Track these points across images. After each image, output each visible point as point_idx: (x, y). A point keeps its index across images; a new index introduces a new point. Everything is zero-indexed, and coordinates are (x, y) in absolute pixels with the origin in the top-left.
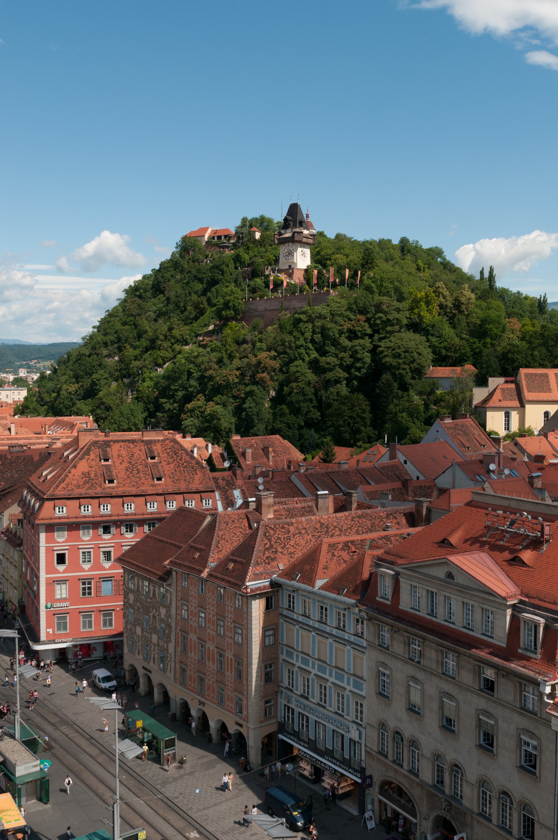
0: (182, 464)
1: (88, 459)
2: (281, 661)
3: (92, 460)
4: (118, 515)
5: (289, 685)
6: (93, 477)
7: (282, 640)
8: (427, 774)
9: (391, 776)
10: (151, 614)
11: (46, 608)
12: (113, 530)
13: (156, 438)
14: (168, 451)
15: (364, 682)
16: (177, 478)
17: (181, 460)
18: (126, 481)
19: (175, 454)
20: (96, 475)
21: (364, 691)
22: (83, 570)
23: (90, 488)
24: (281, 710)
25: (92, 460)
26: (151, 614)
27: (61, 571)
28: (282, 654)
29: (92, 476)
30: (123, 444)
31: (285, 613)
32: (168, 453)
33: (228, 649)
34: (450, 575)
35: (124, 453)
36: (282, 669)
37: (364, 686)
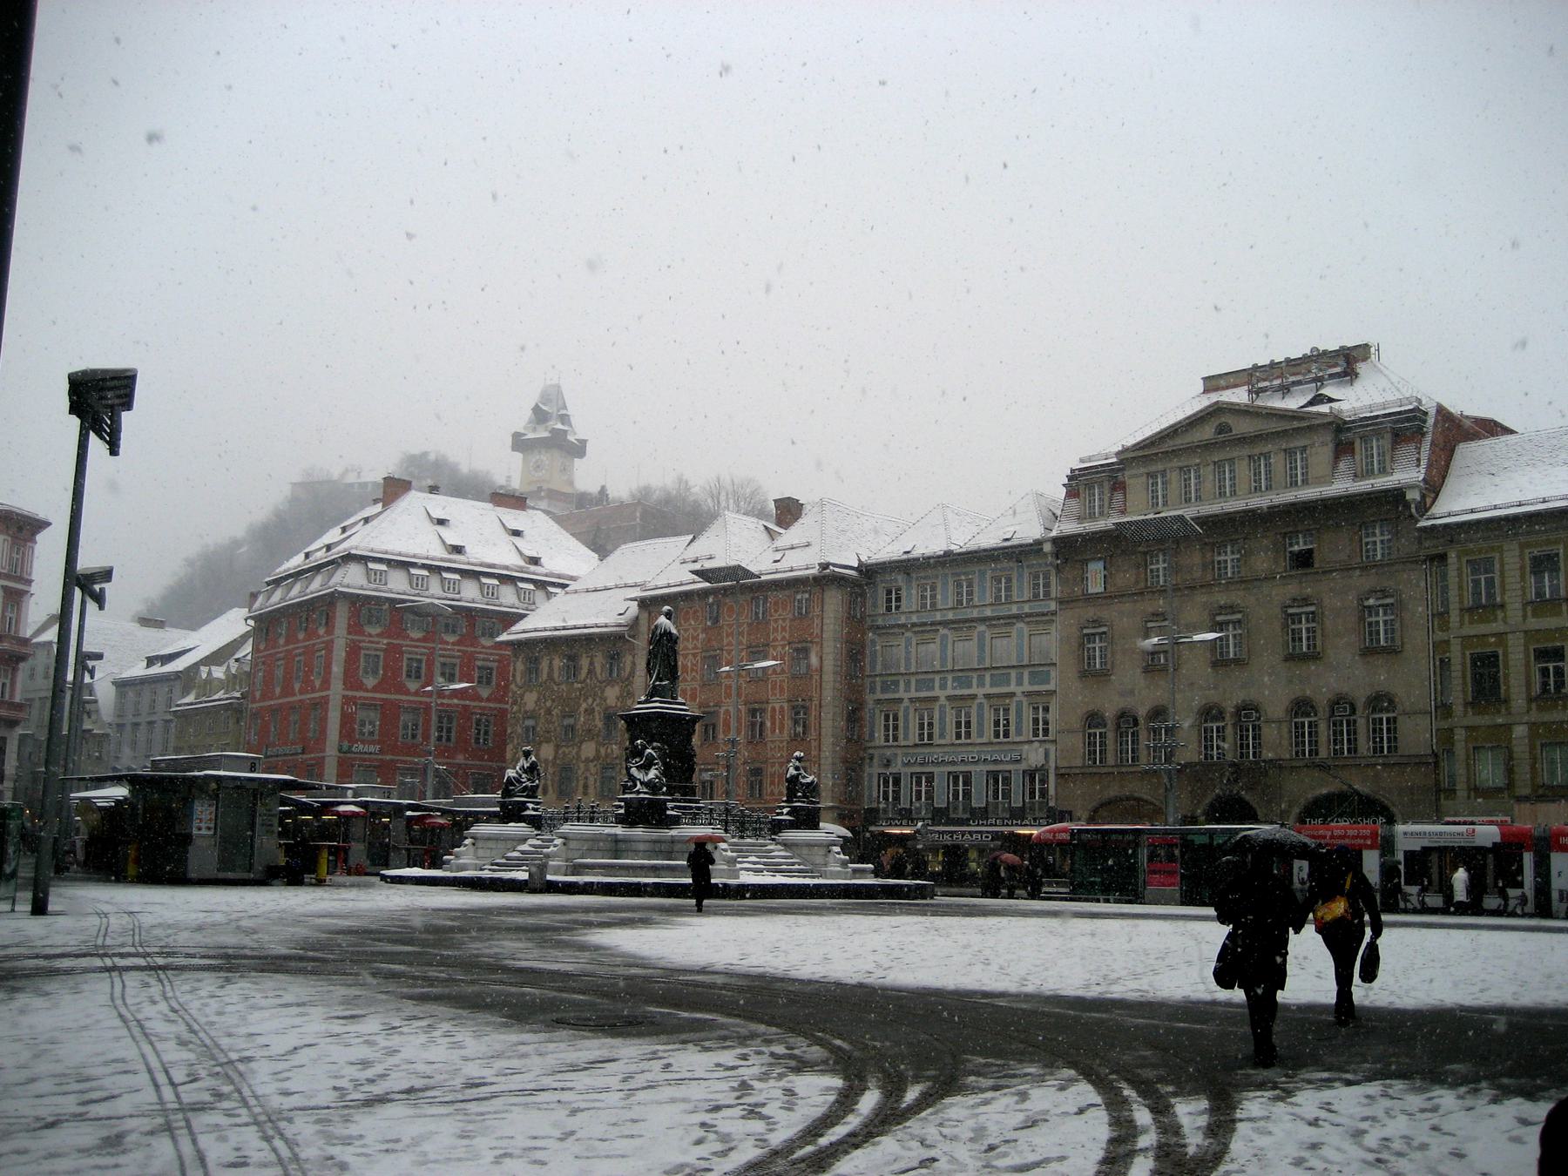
2: (870, 704)
7: (873, 668)
11: (340, 751)
15: (1051, 668)
21: (1053, 682)
22: (407, 692)
24: (870, 788)
28: (873, 690)
34: (1223, 429)
36: (873, 717)
37: (1053, 674)
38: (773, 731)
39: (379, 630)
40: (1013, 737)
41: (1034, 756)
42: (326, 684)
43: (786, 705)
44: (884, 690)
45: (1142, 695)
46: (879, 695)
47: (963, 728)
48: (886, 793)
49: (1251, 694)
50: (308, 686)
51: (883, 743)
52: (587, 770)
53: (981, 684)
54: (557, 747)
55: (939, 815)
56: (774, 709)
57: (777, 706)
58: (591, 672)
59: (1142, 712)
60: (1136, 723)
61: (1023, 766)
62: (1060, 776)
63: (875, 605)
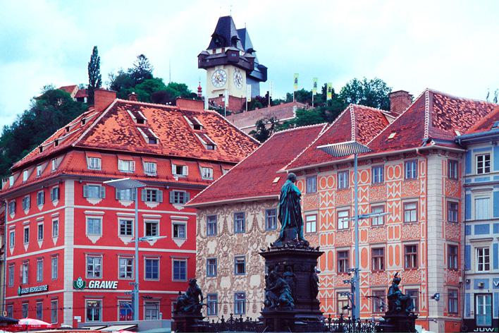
0: (234, 139)
1: (116, 118)
3: (122, 120)
4: (167, 179)
5: (481, 268)
6: (128, 135)
10: (249, 252)
11: (75, 286)
12: (160, 194)
13: (196, 111)
14: (214, 124)
16: (231, 150)
17: (231, 134)
18: (170, 144)
19: (223, 129)
20: (131, 134)
22: (122, 244)
23: (127, 144)
24: (469, 304)
25: (122, 120)
26: (249, 252)
27: (94, 242)
29: (127, 134)
30: (156, 110)
31: (473, 181)
32: (214, 127)
33: (391, 236)
35: (161, 119)
38: (391, 264)
39: (98, 201)
42: (61, 242)
43: (400, 245)
44: (476, 233)
46: (473, 236)
48: (482, 307)
50: (48, 244)
51: (477, 271)
52: (255, 294)
54: (233, 280)
56: (391, 247)
57: (394, 246)
58: (255, 223)
63: (468, 170)
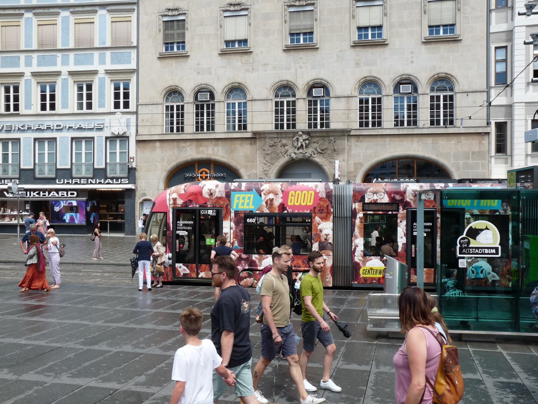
8: (261, 118)
9: (191, 153)
40: (96, 108)
41: (118, 123)
45: (220, 75)
47: (48, 102)
49: (323, 75)
53: (65, 62)
55: (27, 175)
59: (219, 89)
60: (212, 96)
61: (107, 133)
62: (138, 142)
